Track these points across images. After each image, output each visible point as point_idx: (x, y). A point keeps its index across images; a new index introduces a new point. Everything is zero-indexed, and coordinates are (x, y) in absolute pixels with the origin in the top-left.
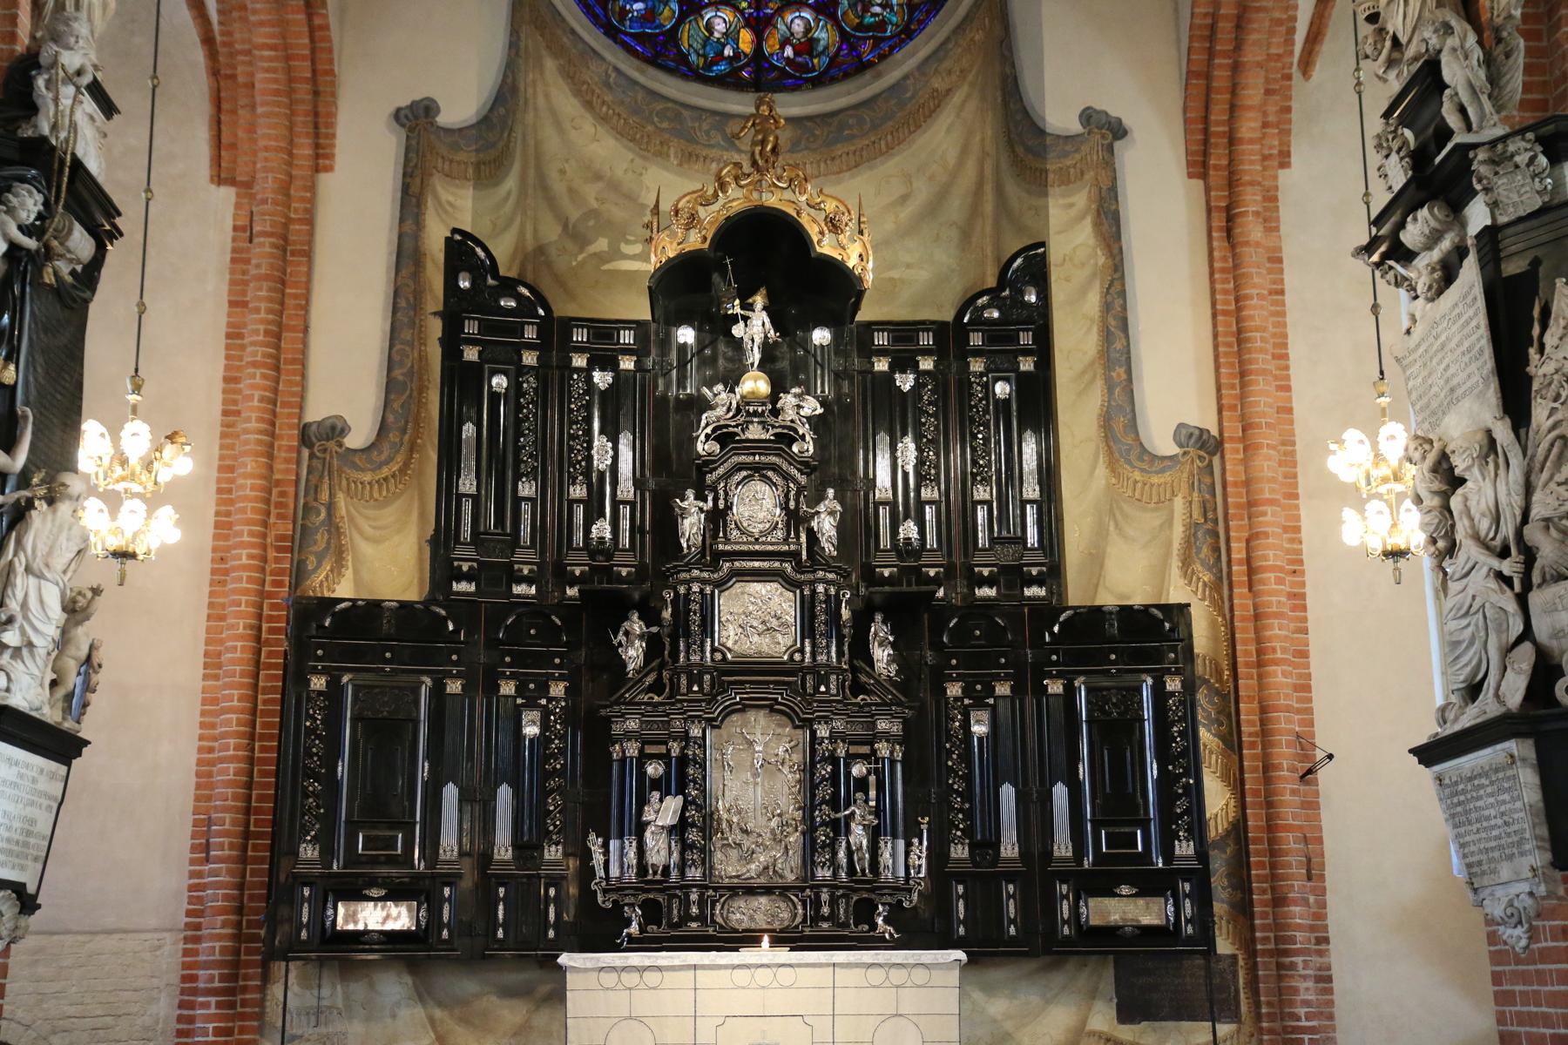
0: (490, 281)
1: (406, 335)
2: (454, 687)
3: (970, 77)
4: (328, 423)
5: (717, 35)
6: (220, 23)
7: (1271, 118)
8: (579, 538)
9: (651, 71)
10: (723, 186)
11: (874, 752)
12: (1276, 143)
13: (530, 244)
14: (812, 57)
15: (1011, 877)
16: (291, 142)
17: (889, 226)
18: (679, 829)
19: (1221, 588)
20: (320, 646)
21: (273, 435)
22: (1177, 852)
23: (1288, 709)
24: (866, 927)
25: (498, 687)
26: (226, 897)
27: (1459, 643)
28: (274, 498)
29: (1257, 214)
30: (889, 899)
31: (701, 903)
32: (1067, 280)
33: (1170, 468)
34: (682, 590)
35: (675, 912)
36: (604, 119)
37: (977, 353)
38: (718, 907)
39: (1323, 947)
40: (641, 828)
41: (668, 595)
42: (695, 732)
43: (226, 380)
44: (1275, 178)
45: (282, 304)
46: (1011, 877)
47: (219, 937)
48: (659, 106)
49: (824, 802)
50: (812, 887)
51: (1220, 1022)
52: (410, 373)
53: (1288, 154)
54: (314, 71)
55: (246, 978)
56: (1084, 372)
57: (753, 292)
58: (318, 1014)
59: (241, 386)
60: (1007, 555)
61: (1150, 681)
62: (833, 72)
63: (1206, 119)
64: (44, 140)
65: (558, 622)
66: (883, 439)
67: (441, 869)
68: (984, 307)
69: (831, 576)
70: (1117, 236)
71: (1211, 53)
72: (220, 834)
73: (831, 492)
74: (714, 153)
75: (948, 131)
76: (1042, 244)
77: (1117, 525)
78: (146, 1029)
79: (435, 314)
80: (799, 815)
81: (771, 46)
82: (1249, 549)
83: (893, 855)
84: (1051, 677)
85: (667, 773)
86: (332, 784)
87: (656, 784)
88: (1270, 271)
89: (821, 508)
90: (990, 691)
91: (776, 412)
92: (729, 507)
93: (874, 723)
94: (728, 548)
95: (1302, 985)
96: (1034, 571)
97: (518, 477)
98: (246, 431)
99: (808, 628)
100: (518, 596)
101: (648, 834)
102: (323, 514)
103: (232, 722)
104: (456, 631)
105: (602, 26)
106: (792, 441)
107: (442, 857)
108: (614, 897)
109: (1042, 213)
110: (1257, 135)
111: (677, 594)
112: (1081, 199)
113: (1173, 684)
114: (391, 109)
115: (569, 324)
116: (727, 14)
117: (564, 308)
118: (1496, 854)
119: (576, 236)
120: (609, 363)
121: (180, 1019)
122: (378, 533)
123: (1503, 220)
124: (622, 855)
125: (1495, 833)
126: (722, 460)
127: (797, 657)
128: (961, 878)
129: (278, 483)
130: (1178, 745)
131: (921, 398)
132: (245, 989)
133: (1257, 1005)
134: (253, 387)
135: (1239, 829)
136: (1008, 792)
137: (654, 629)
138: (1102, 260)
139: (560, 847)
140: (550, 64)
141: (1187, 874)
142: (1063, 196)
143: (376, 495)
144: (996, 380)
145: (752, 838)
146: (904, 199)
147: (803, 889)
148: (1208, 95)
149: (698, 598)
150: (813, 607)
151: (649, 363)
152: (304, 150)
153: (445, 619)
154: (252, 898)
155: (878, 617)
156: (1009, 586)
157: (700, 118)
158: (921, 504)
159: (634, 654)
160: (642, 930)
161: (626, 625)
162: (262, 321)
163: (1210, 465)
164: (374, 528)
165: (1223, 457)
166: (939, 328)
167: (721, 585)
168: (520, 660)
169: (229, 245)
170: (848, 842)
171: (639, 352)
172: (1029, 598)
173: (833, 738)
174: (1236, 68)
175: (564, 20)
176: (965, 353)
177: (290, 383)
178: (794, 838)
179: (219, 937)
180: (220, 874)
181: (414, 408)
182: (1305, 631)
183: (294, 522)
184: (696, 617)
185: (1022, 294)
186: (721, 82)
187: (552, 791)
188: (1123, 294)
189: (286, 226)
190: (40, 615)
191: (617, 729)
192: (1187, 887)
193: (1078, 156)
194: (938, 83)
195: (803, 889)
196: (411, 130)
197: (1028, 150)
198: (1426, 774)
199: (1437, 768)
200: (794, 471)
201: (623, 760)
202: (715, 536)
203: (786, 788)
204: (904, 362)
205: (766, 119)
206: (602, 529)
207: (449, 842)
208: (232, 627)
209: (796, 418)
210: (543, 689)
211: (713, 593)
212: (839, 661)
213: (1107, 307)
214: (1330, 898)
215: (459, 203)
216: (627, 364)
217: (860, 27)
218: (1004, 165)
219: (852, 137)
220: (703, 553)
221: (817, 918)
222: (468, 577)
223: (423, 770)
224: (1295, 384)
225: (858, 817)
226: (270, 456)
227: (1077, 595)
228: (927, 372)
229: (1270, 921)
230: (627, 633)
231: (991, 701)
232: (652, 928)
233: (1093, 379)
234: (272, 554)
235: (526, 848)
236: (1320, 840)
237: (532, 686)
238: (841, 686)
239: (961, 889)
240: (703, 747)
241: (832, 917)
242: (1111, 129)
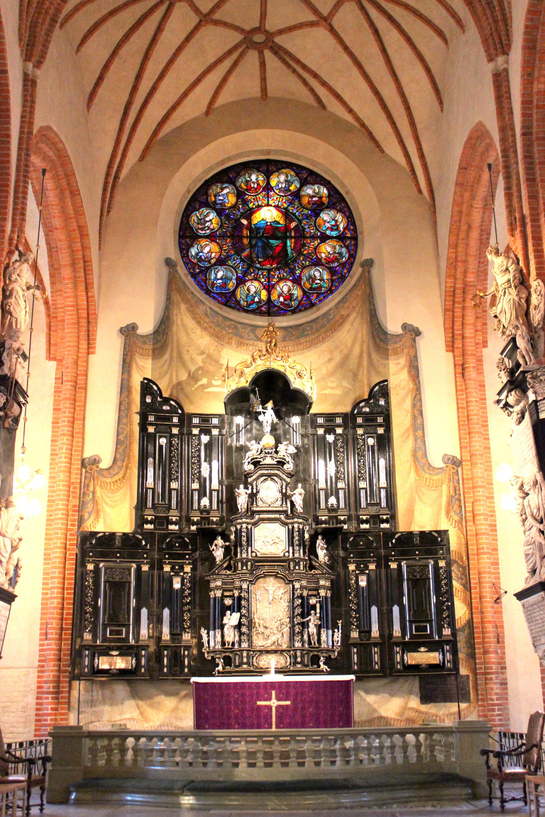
0: (159, 399)
1: (124, 421)
2: (145, 568)
3: (357, 309)
4: (93, 458)
5: (252, 293)
6: (52, 296)
7: (479, 328)
8: (196, 506)
9: (225, 308)
10: (254, 360)
11: (319, 594)
12: (481, 338)
13: (175, 381)
14: (291, 301)
15: (375, 645)
16: (79, 343)
17: (324, 371)
18: (239, 626)
19: (462, 523)
20: (91, 552)
21: (71, 463)
22: (444, 633)
23: (490, 573)
24: (316, 666)
25: (163, 568)
26: (54, 654)
27: (528, 555)
28: (71, 490)
29: (474, 367)
30: (325, 655)
31: (248, 657)
32: (397, 394)
33: (440, 473)
34: (239, 527)
35: (237, 661)
36: (205, 329)
37: (360, 426)
38: (255, 658)
39: (504, 671)
40: (222, 627)
41: (233, 529)
42: (245, 586)
43: (52, 441)
44: (481, 352)
45: (75, 409)
46: (375, 645)
47: (52, 671)
48: (228, 323)
49: (298, 615)
50: (293, 650)
51: (462, 702)
52: (126, 437)
53: (487, 342)
54: (88, 314)
55: (63, 687)
56: (405, 433)
57: (267, 402)
58: (92, 703)
59: (58, 443)
60: (373, 510)
61: (432, 562)
62: (300, 307)
63: (453, 328)
64: (6, 375)
65: (188, 541)
66: (321, 462)
67: (140, 643)
68: (363, 407)
69: (301, 520)
70: (418, 376)
71: (454, 302)
72: (52, 628)
73: (300, 485)
74: (251, 342)
75: (349, 331)
76: (386, 381)
77: (419, 497)
78: (24, 707)
79: (137, 413)
80: (288, 620)
81: (274, 297)
82: (473, 506)
83: (327, 636)
84: (392, 561)
85: (233, 603)
86: (96, 608)
87: (229, 608)
88: (480, 390)
89: (296, 491)
90: (367, 567)
91: (277, 452)
92: (258, 492)
93: (318, 582)
94: (258, 509)
95: (495, 686)
96: (385, 517)
97: (170, 480)
98: (61, 463)
99: (291, 542)
100: (171, 530)
101: (225, 629)
102: (91, 496)
103: (57, 582)
104: (146, 545)
105: (204, 290)
106: (284, 464)
107: (141, 638)
108: (212, 655)
109: (386, 366)
110: (473, 335)
111: (236, 528)
112: (403, 361)
113: (442, 564)
114: (119, 328)
115: (191, 416)
116: (256, 284)
117: (189, 409)
118: (540, 633)
119: (193, 377)
120: (207, 432)
121: (37, 704)
122: (113, 504)
123: (539, 398)
124: (215, 637)
125: (540, 625)
126: (255, 472)
127: (287, 554)
128: (355, 645)
129: (73, 483)
130: (444, 589)
131: (337, 445)
132: (62, 692)
133: (477, 695)
134: (63, 444)
135: (470, 623)
136: (374, 610)
137: (227, 544)
138: (411, 386)
139: (189, 634)
140: (183, 306)
141: (448, 642)
142: (395, 360)
143: (112, 488)
144: (368, 437)
145: (268, 630)
146: (330, 360)
147: (289, 651)
148: (453, 318)
149: (244, 530)
150: (293, 533)
151: (224, 432)
152: (84, 345)
153: (141, 540)
154: (64, 655)
155: (320, 537)
156: (375, 523)
157: (245, 328)
158: (337, 490)
159: (219, 554)
160: (224, 668)
161: (216, 542)
162: (66, 417)
163: (457, 471)
164: (112, 501)
165: (462, 468)
167: (255, 524)
168: (172, 556)
169: (53, 386)
170: (308, 631)
171: (220, 427)
172: (383, 529)
173: (302, 588)
174: (464, 308)
175: (189, 289)
176: (356, 426)
177: (78, 442)
178: (286, 630)
179: (52, 671)
180: (52, 645)
181: (128, 452)
182: (496, 540)
183: (80, 499)
184: (244, 539)
185: (378, 401)
186: (253, 312)
187: (186, 611)
188: (420, 400)
189: (76, 377)
190: (4, 550)
191: (212, 585)
192: (448, 647)
193: (401, 343)
194: (343, 312)
195: (289, 651)
196: (126, 336)
197: (381, 340)
198: (518, 604)
199: (523, 601)
200: (284, 477)
201: (215, 598)
202: (252, 504)
203: (282, 610)
204: (330, 430)
205: (271, 332)
206: (205, 501)
207: (144, 632)
208: (54, 543)
209: (285, 454)
210: (182, 568)
211: (251, 528)
212: (304, 556)
213: (414, 406)
214: (507, 651)
215: (146, 366)
216: (215, 432)
217: (311, 289)
218: (371, 345)
219: (308, 335)
220: (247, 511)
221: (295, 663)
222: (151, 522)
223: (133, 603)
224: (491, 437)
225: (312, 619)
226: (70, 472)
227: (402, 527)
228: (340, 435)
229: (482, 660)
230: (216, 545)
231: (367, 572)
232: (228, 668)
233: (408, 436)
234: (71, 513)
235: (175, 635)
236: (502, 627)
237: (177, 567)
238: (305, 566)
239: (355, 650)
240: (248, 592)
241: (302, 662)
242: (414, 331)
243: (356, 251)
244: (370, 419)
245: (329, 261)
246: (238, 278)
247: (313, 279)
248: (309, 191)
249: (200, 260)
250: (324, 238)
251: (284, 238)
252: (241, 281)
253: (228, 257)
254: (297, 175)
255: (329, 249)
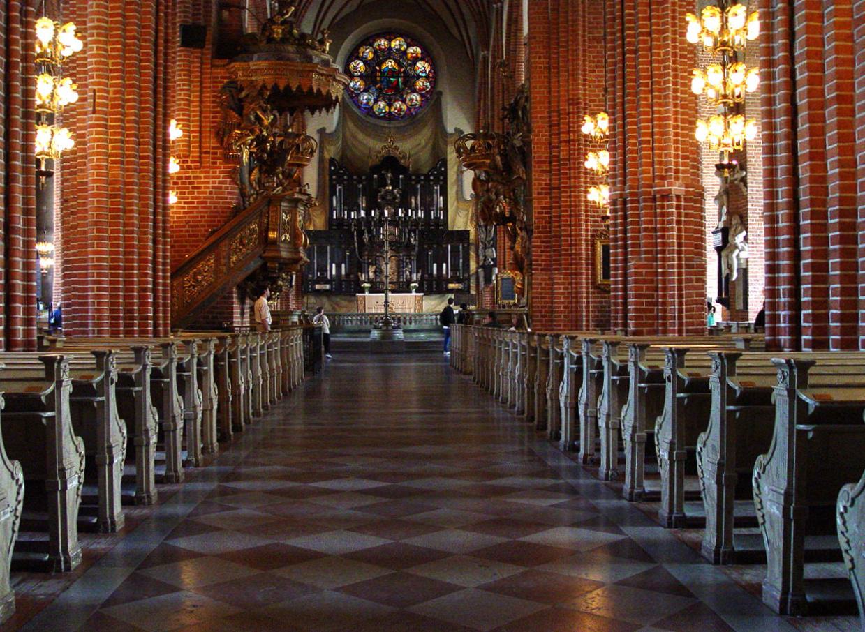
9: (368, 116)
40: (368, 272)
81: (392, 110)
120: (359, 182)
136: (435, 265)
141: (466, 279)
166: (424, 175)
173: (404, 255)
204: (418, 182)
223: (329, 261)
227: (450, 229)
243: (435, 85)
244: (436, 177)
245: (421, 90)
246: (374, 100)
247: (412, 100)
248: (411, 50)
249: (355, 89)
250: (419, 77)
251: (398, 77)
252: (376, 101)
253: (369, 88)
254: (405, 41)
255: (421, 84)
